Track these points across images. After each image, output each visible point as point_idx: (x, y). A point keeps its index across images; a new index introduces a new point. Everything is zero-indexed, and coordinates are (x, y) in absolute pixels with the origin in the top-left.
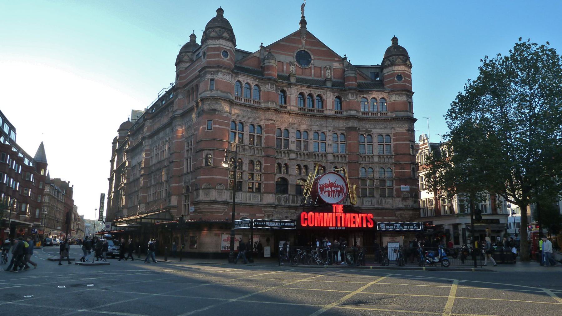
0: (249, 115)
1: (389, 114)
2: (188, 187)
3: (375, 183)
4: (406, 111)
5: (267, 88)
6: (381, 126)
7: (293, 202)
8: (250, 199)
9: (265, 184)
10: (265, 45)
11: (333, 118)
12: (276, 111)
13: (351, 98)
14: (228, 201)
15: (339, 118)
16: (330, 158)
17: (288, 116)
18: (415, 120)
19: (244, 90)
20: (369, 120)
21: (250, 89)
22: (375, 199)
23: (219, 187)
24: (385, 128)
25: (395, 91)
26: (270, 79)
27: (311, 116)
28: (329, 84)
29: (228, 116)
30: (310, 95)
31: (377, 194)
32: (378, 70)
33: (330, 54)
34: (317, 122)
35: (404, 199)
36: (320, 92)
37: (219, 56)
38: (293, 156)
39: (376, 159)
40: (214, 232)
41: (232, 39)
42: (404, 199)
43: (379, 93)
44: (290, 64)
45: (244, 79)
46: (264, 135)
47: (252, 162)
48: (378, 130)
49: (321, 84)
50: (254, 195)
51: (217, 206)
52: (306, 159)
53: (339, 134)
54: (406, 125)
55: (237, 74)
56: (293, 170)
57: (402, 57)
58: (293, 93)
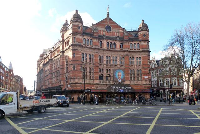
0: (89, 51)
1: (140, 50)
2: (67, 78)
4: (147, 48)
5: (95, 40)
6: (138, 54)
7: (105, 82)
10: (94, 24)
11: (120, 51)
12: (98, 49)
13: (126, 44)
14: (82, 82)
15: (122, 51)
16: (119, 66)
17: (103, 51)
18: (150, 52)
19: (87, 42)
20: (133, 52)
21: (89, 41)
23: (79, 78)
24: (139, 55)
25: (143, 41)
26: (96, 37)
27: (111, 51)
28: (118, 39)
30: (111, 43)
31: (136, 79)
32: (136, 33)
33: (118, 27)
34: (114, 53)
35: (146, 81)
36: (115, 42)
37: (77, 29)
38: (105, 66)
41: (81, 22)
42: (146, 81)
43: (137, 42)
44: (104, 31)
45: (86, 37)
46: (94, 58)
48: (137, 55)
49: (115, 39)
52: (110, 67)
54: (147, 53)
55: (84, 35)
56: (105, 71)
57: (145, 28)
58: (105, 42)
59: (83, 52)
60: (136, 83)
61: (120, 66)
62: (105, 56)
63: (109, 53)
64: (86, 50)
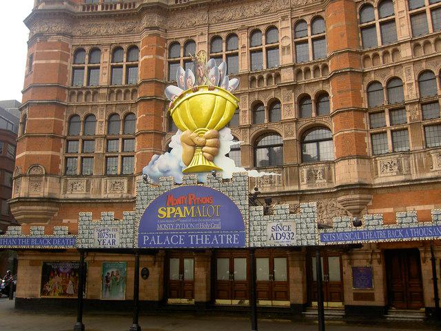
0: (111, 31)
3: (408, 115)
9: (138, 156)
16: (287, 76)
39: (406, 52)
40: (29, 258)
47: (111, 118)
50: (114, 180)
51: (28, 207)
53: (308, 19)
59: (78, 42)
60: (423, 167)
61: (298, 73)
62: (205, 38)
63: (229, 15)
64: (94, 30)
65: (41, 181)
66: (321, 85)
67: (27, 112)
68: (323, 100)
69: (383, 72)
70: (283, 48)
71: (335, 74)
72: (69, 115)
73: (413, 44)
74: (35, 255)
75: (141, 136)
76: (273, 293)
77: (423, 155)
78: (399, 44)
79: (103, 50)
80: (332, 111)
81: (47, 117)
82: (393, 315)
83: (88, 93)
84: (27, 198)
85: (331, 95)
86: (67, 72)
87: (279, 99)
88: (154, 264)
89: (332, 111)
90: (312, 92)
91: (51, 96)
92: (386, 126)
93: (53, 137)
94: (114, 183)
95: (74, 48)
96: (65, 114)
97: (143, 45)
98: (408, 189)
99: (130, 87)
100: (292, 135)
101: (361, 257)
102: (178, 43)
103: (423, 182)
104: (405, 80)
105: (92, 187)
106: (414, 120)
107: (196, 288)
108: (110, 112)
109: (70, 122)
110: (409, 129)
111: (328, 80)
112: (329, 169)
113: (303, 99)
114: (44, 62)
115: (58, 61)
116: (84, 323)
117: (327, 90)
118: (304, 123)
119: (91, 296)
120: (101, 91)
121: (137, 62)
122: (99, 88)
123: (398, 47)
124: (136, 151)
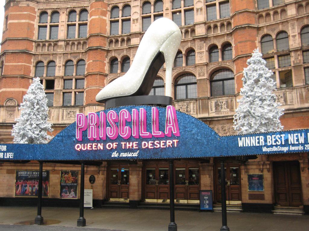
3: (292, 59)
8: (63, 118)
9: (86, 92)
16: (200, 31)
22: (295, 91)
29: (28, 5)
40: (6, 168)
50: (69, 110)
51: (5, 130)
59: (43, 7)
61: (209, 28)
65: (14, 111)
66: (226, 37)
67: (4, 59)
68: (227, 49)
69: (273, 27)
70: (197, 10)
71: (236, 29)
72: (35, 61)
73: (297, 5)
74: (11, 166)
75: (89, 77)
76: (188, 194)
77: (303, 90)
78: (286, 5)
79: (61, 13)
80: (234, 57)
81: (19, 62)
82: (278, 212)
83: (50, 45)
84: (4, 123)
85: (233, 45)
86: (34, 29)
87: (194, 48)
88: (99, 173)
89: (234, 57)
90: (219, 43)
91: (21, 46)
92: (275, 68)
93: (23, 78)
94: (69, 112)
95: (40, 11)
96: (32, 60)
97: (91, 8)
98: (291, 115)
99: (81, 40)
100: (204, 75)
101: (254, 167)
102: (117, 7)
103: (303, 110)
104: (290, 33)
105: (52, 115)
106: (297, 63)
107: (131, 191)
108: (66, 59)
109: (36, 67)
110: (293, 71)
111: (231, 34)
112: (232, 101)
113: (212, 48)
114: (16, 21)
115: (27, 21)
116: (42, 216)
117: (230, 42)
118: (212, 67)
119: (53, 196)
120: (60, 43)
121: (87, 22)
122: (58, 41)
123: (285, 8)
124: (85, 88)
